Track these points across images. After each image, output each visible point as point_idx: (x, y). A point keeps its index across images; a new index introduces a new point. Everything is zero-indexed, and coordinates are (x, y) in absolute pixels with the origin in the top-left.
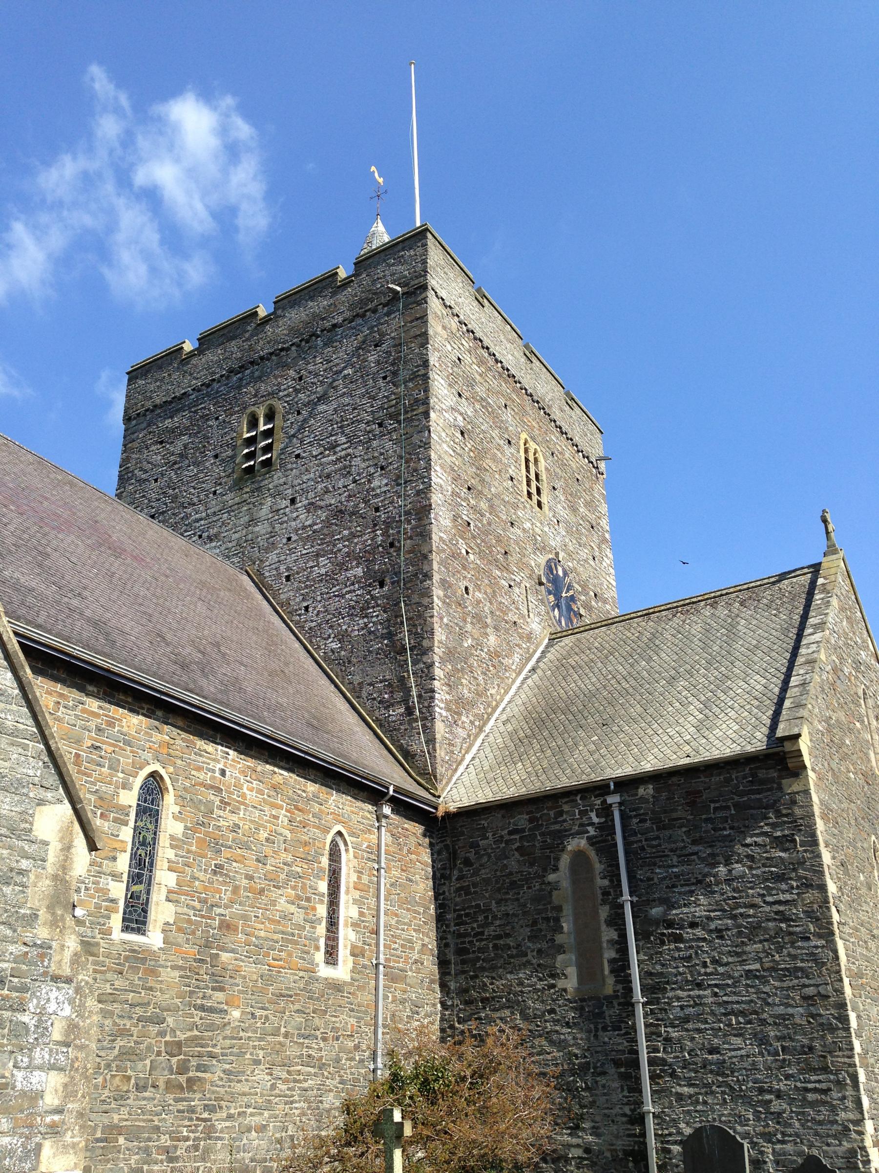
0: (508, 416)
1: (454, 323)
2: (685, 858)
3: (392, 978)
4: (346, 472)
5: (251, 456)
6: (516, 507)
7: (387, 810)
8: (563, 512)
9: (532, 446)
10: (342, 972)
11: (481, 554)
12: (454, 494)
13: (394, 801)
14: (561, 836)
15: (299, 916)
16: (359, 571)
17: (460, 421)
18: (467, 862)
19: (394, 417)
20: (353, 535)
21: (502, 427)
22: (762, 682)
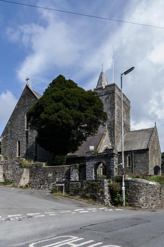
8: (126, 116)
22: (147, 142)
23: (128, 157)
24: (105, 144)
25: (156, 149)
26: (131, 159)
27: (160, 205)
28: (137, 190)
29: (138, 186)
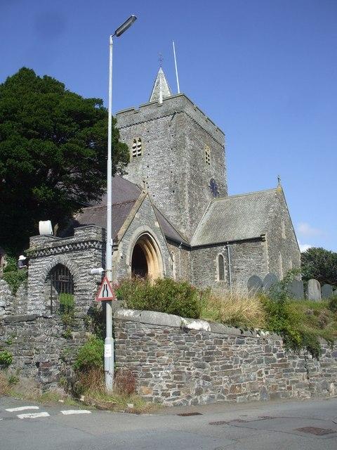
4: (163, 161)
5: (134, 152)
14: (216, 253)
23: (217, 258)
24: (140, 225)
25: (285, 237)
27: (225, 392)
28: (148, 349)
29: (152, 335)
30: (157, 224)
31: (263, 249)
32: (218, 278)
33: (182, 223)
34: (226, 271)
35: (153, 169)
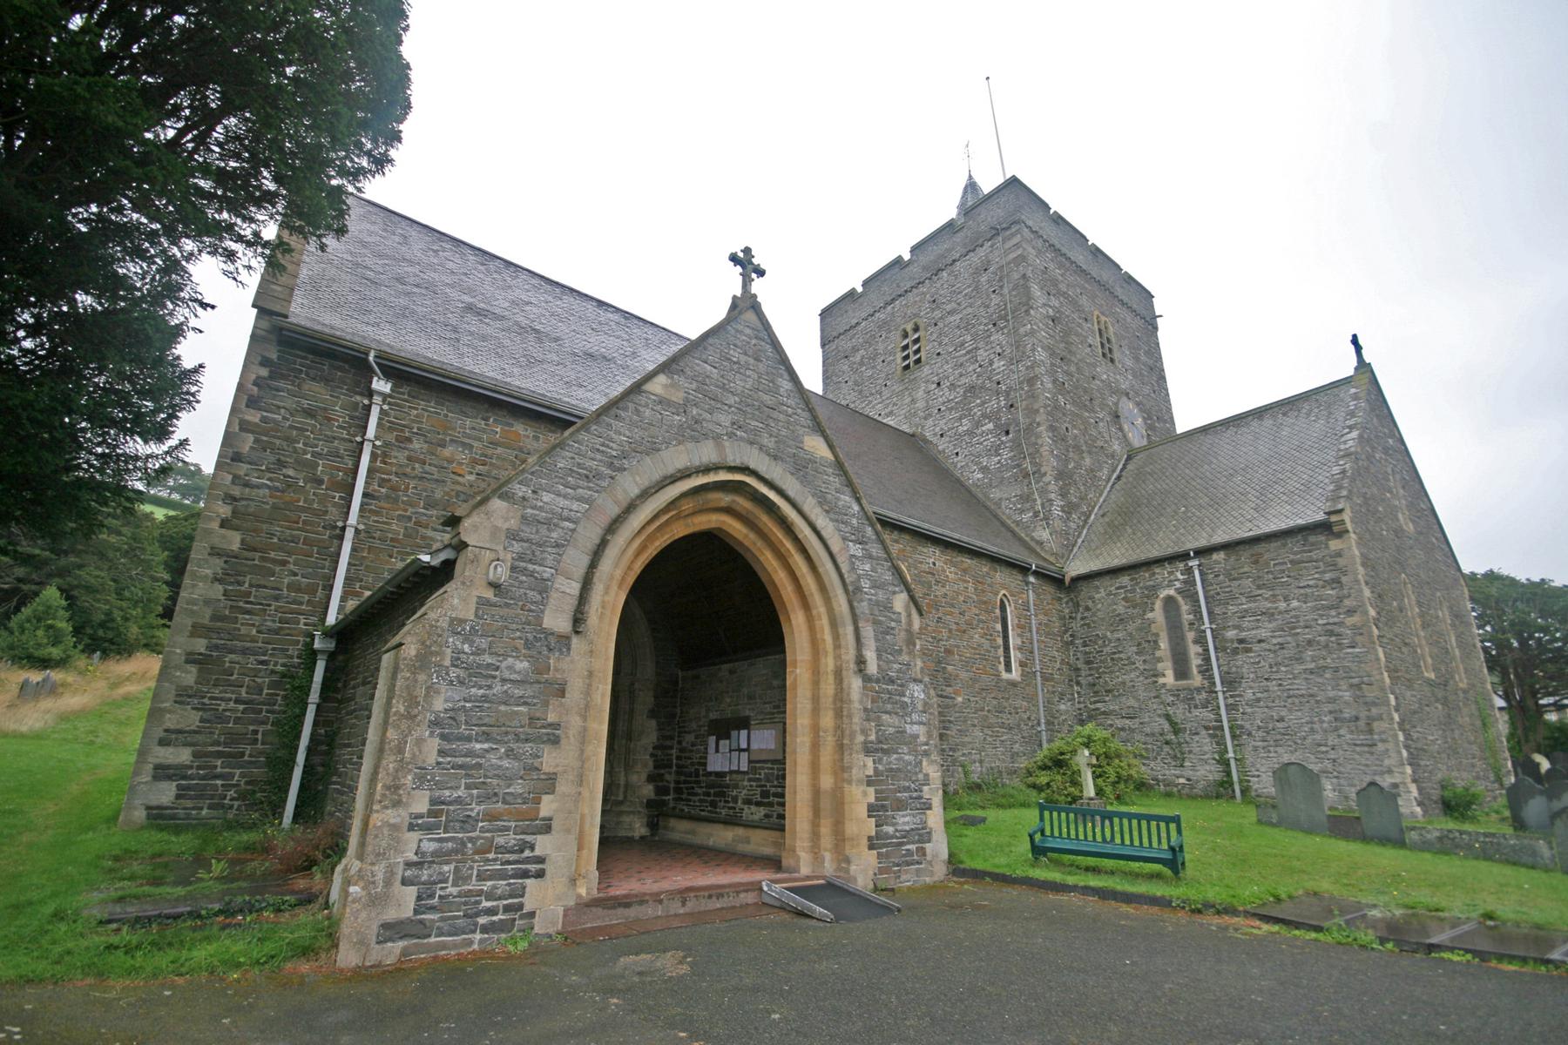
0: (1084, 301)
1: (1040, 243)
2: (1252, 598)
3: (1045, 679)
5: (907, 357)
6: (1095, 366)
7: (1032, 579)
8: (1129, 363)
9: (1103, 318)
10: (1015, 674)
11: (1074, 403)
12: (1052, 365)
13: (1036, 573)
14: (1154, 589)
15: (986, 645)
16: (991, 426)
17: (1051, 312)
18: (1087, 609)
19: (1004, 318)
20: (983, 403)
21: (1078, 308)
23: (1158, 605)
24: (693, 432)
26: (1187, 617)
30: (816, 446)
31: (1341, 562)
32: (1170, 673)
33: (1036, 514)
34: (1194, 650)
35: (953, 386)
